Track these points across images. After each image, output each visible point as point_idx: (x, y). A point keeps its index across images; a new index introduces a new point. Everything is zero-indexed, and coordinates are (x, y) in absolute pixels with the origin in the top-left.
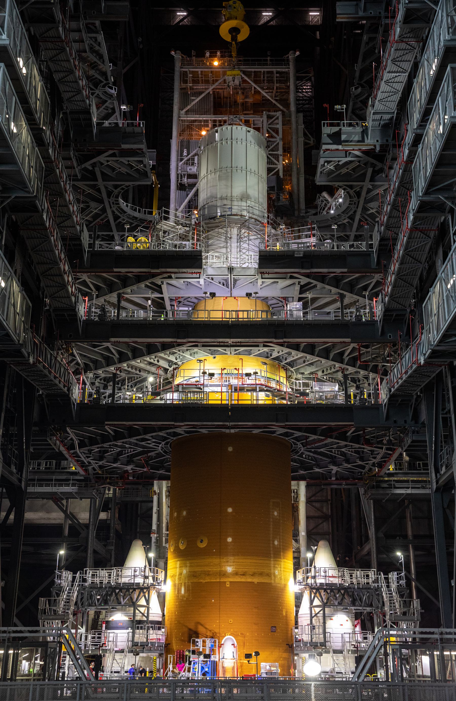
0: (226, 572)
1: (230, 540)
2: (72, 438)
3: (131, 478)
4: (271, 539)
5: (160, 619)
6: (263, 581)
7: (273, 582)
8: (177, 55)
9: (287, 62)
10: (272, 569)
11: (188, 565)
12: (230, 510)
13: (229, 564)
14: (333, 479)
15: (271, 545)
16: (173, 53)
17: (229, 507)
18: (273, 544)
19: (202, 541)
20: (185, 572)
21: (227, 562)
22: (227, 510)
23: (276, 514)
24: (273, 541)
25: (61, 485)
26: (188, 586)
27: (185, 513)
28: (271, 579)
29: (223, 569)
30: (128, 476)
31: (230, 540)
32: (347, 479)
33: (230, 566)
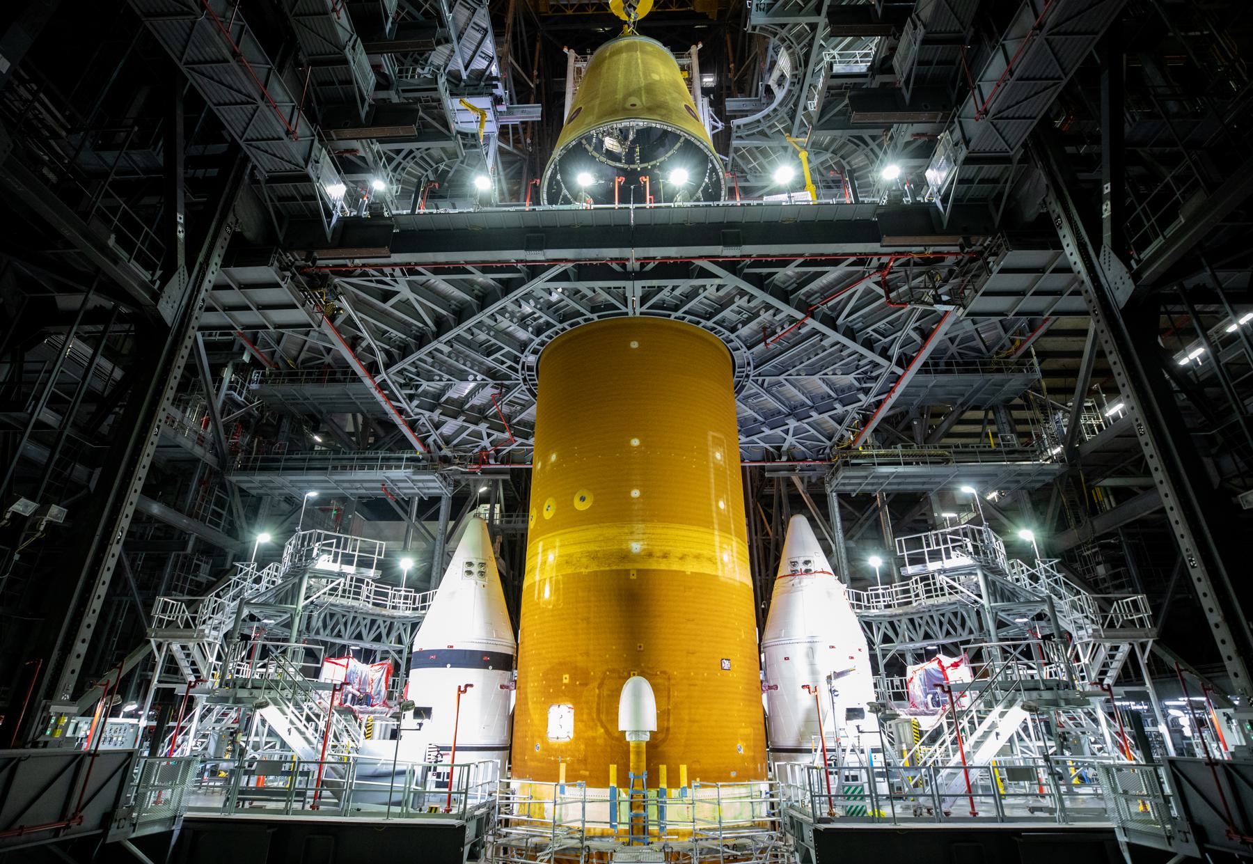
0: (629, 551)
1: (635, 493)
2: (369, 346)
3: (492, 461)
4: (713, 497)
5: (510, 651)
6: (701, 571)
7: (720, 574)
8: (571, 54)
9: (690, 56)
10: (717, 549)
11: (558, 544)
12: (635, 442)
13: (637, 537)
14: (784, 458)
15: (714, 508)
16: (565, 50)
17: (634, 437)
18: (717, 507)
19: (583, 499)
20: (552, 557)
21: (632, 533)
22: (629, 442)
23: (718, 456)
24: (717, 502)
25: (389, 468)
26: (557, 582)
27: (553, 457)
28: (717, 569)
29: (624, 547)
30: (488, 457)
31: (635, 493)
32: (805, 460)
33: (638, 540)
